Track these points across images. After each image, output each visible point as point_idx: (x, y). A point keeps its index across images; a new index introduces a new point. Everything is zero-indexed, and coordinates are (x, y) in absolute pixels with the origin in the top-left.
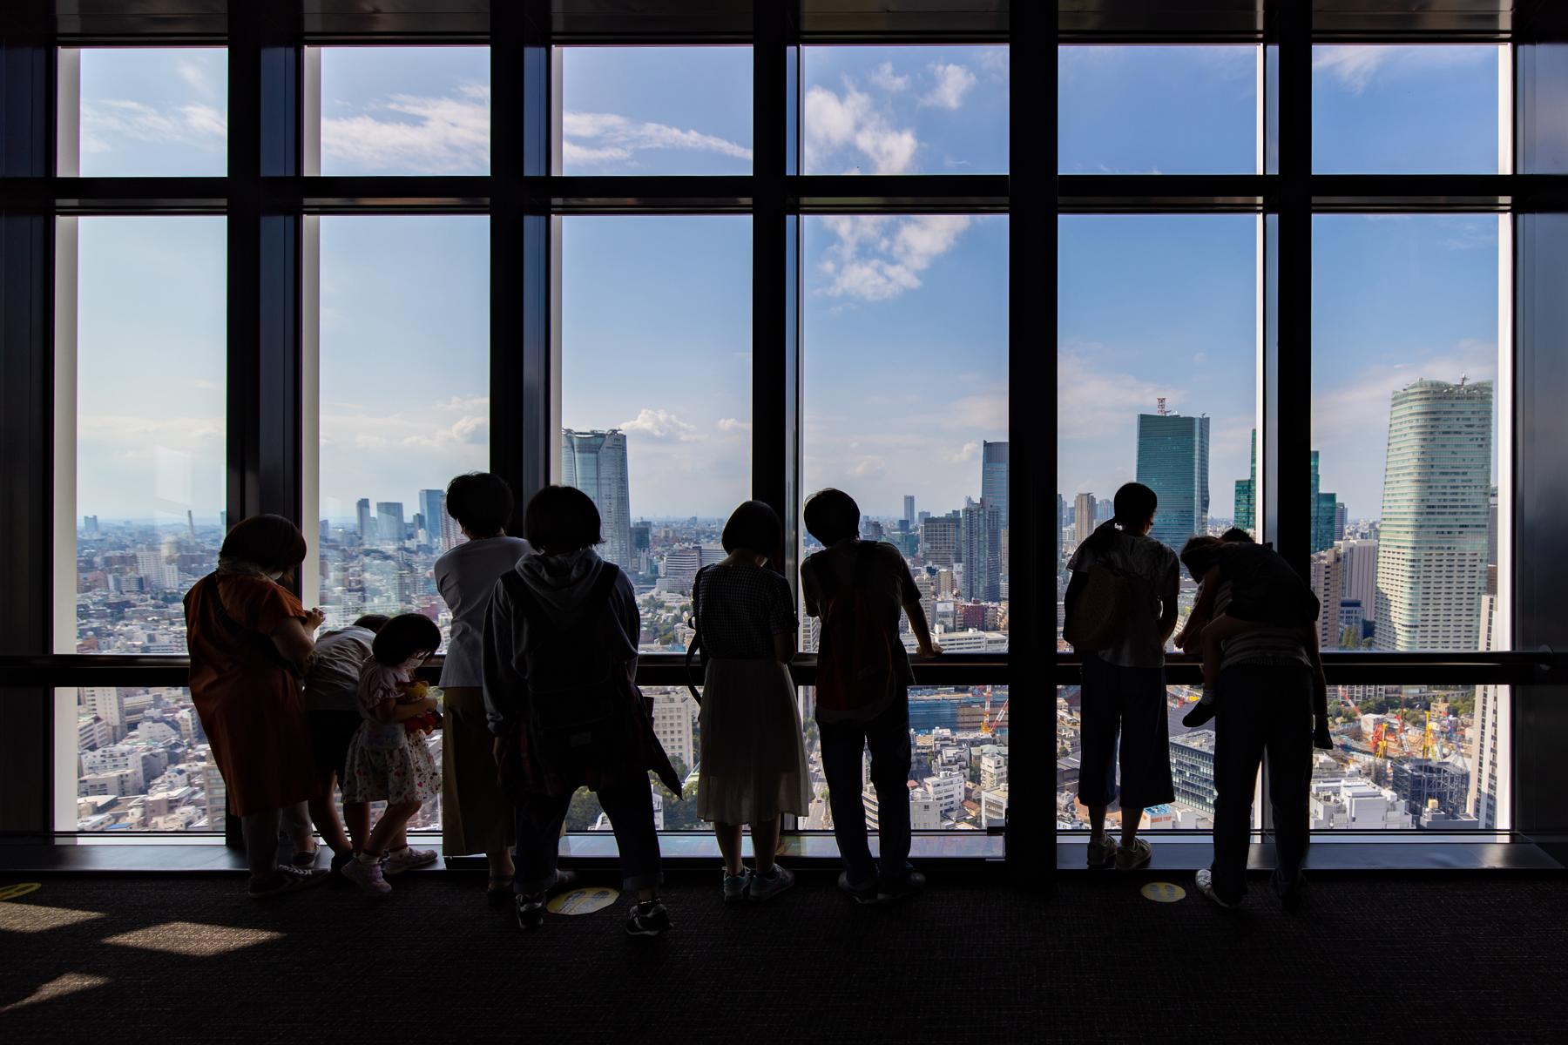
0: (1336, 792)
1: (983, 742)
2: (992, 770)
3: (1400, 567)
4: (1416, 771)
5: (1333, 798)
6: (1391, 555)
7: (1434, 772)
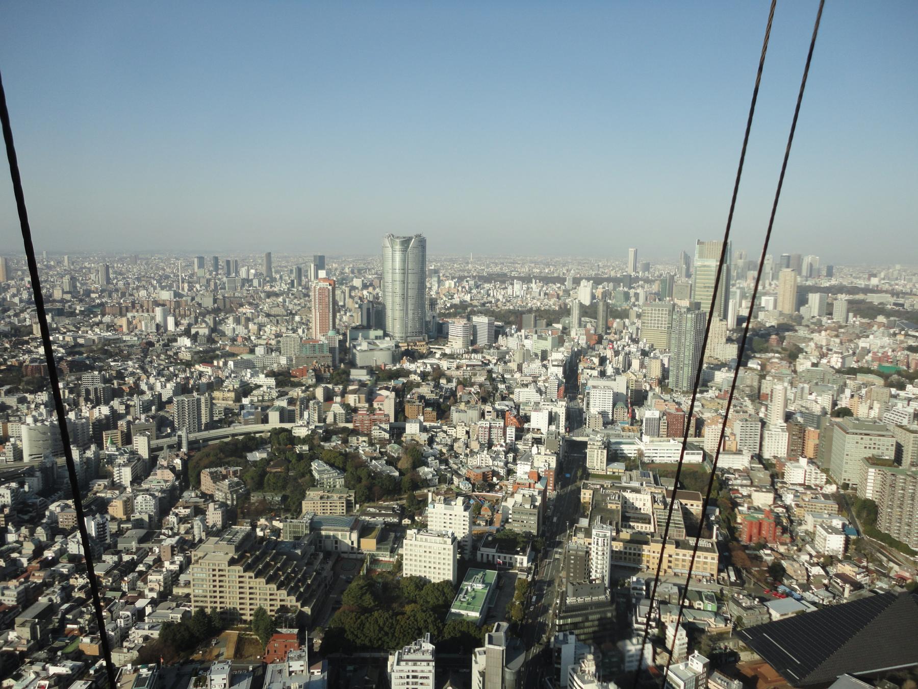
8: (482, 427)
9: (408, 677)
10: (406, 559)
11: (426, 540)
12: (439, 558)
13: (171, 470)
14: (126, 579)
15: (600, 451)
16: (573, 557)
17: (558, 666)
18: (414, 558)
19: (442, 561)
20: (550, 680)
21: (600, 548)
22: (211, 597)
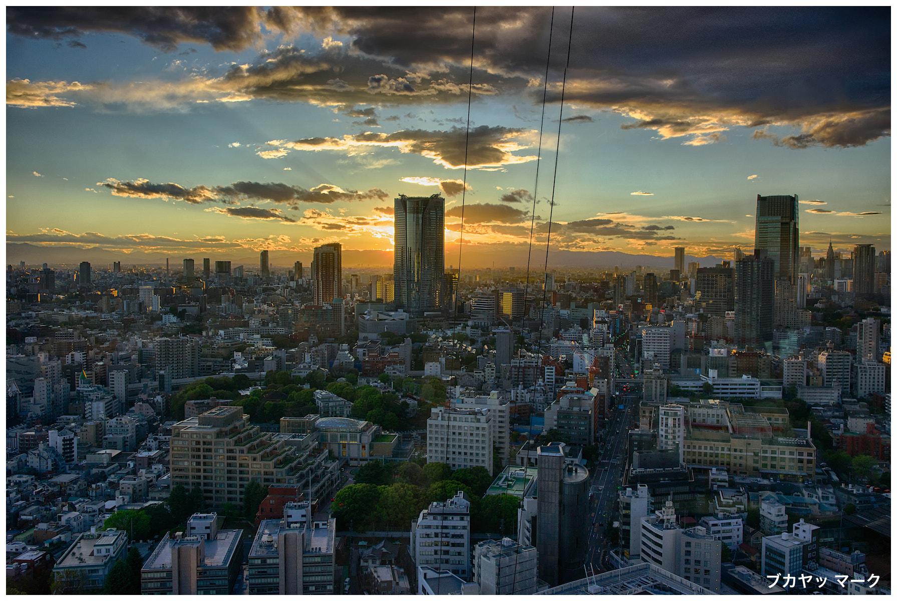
8: (515, 367)
9: (436, 535)
10: (431, 438)
12: (472, 441)
13: (150, 404)
14: (94, 486)
15: (659, 381)
16: (636, 443)
17: (627, 528)
19: (475, 445)
20: (617, 553)
21: (670, 431)
22: (194, 477)
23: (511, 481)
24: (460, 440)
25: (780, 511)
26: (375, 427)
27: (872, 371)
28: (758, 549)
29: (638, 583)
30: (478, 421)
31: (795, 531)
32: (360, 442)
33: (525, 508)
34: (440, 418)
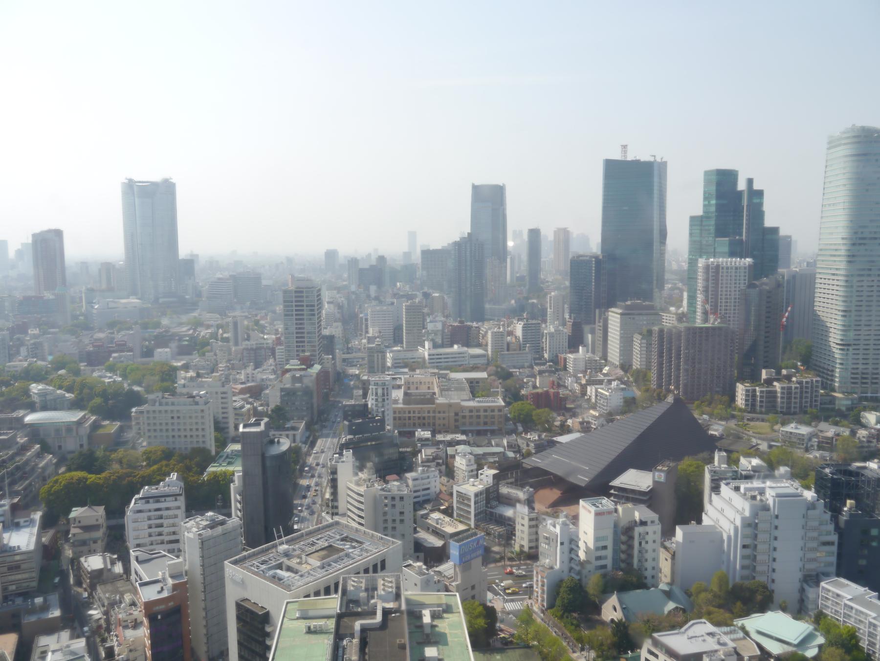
0: (762, 492)
1: (459, 443)
2: (464, 468)
3: (835, 292)
4: (835, 475)
5: (758, 498)
6: (827, 281)
7: (853, 476)
11: (173, 404)
15: (380, 355)
18: (158, 427)
23: (232, 458)
24: (179, 424)
25: (470, 461)
26: (94, 418)
27: (558, 336)
28: (451, 494)
29: (326, 538)
30: (197, 403)
31: (480, 477)
32: (77, 433)
33: (236, 482)
34: (157, 404)
